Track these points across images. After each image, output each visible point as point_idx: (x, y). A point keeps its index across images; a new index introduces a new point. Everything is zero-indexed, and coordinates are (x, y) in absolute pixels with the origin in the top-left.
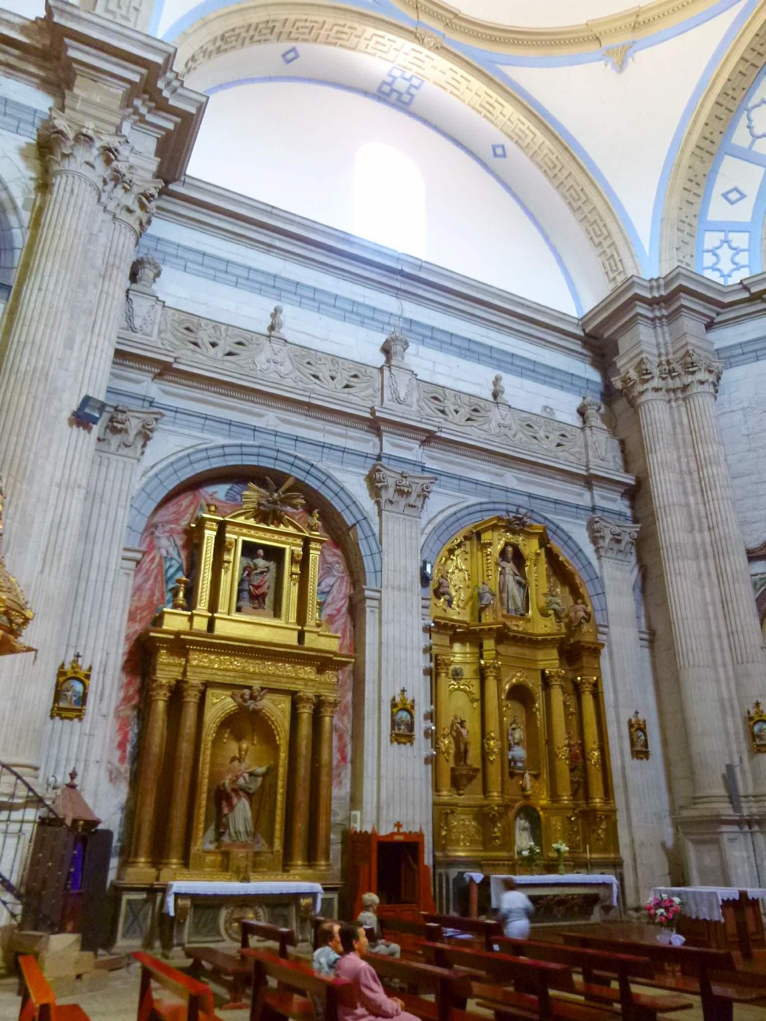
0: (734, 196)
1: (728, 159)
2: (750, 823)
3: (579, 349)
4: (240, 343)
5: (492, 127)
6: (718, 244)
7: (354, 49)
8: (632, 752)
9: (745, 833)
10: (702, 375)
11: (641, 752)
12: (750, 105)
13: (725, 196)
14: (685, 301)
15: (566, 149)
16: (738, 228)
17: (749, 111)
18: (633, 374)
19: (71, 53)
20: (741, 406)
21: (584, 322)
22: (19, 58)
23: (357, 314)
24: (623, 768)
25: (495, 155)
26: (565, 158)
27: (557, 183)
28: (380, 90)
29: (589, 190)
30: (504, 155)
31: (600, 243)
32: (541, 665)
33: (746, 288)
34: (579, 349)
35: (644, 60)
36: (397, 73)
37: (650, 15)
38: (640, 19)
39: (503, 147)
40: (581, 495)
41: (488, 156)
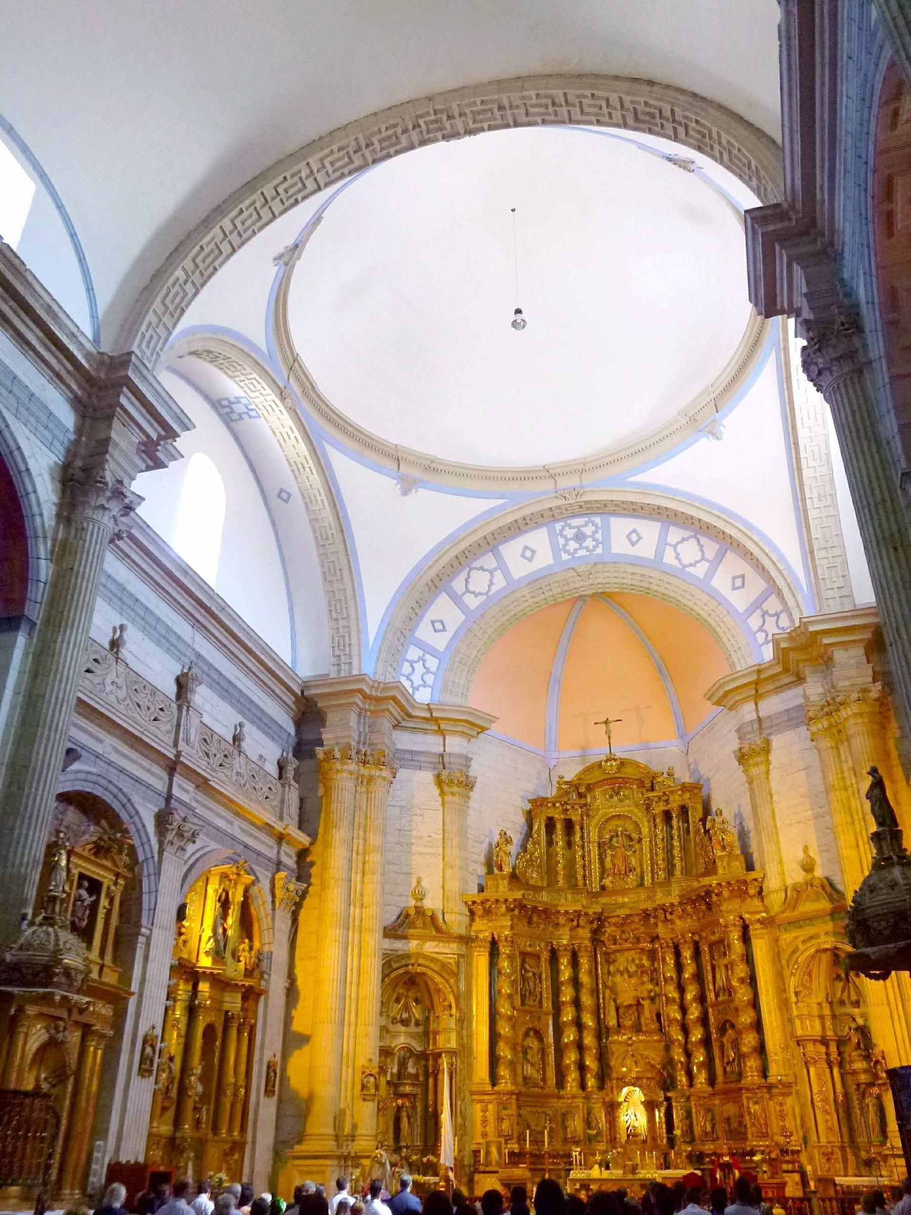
0: (439, 626)
1: (444, 595)
2: (346, 1158)
3: (290, 703)
4: (96, 660)
5: (294, 482)
6: (416, 658)
7: (231, 377)
8: (266, 1091)
9: (340, 1166)
10: (386, 773)
11: (269, 1092)
12: (474, 565)
13: (433, 622)
14: (391, 706)
15: (342, 531)
16: (433, 652)
17: (471, 569)
18: (338, 755)
19: (123, 400)
20: (400, 804)
21: (305, 686)
22: (68, 372)
23: (168, 640)
24: (257, 1104)
25: (279, 496)
26: (338, 538)
27: (322, 551)
28: (219, 401)
29: (346, 572)
30: (286, 501)
31: (337, 619)
32: (227, 1006)
33: (430, 710)
34: (290, 703)
35: (423, 497)
36: (244, 401)
37: (440, 467)
38: (432, 465)
39: (289, 495)
40: (271, 848)
41: (272, 494)
